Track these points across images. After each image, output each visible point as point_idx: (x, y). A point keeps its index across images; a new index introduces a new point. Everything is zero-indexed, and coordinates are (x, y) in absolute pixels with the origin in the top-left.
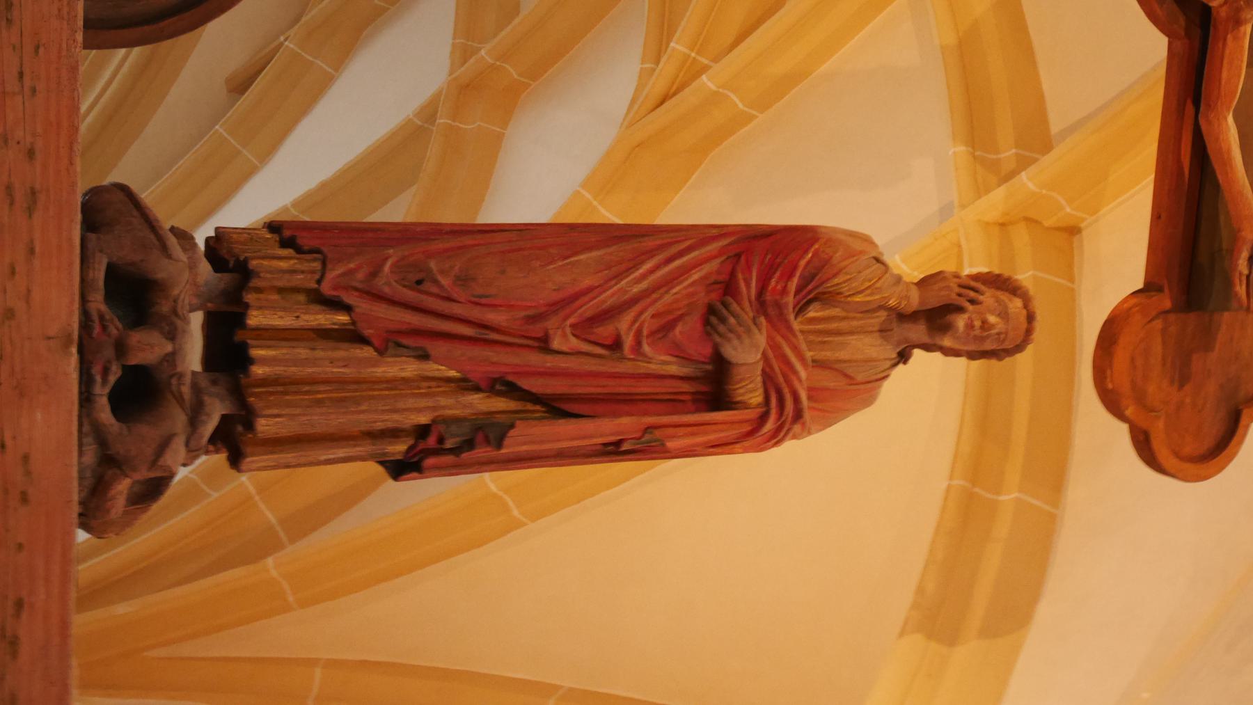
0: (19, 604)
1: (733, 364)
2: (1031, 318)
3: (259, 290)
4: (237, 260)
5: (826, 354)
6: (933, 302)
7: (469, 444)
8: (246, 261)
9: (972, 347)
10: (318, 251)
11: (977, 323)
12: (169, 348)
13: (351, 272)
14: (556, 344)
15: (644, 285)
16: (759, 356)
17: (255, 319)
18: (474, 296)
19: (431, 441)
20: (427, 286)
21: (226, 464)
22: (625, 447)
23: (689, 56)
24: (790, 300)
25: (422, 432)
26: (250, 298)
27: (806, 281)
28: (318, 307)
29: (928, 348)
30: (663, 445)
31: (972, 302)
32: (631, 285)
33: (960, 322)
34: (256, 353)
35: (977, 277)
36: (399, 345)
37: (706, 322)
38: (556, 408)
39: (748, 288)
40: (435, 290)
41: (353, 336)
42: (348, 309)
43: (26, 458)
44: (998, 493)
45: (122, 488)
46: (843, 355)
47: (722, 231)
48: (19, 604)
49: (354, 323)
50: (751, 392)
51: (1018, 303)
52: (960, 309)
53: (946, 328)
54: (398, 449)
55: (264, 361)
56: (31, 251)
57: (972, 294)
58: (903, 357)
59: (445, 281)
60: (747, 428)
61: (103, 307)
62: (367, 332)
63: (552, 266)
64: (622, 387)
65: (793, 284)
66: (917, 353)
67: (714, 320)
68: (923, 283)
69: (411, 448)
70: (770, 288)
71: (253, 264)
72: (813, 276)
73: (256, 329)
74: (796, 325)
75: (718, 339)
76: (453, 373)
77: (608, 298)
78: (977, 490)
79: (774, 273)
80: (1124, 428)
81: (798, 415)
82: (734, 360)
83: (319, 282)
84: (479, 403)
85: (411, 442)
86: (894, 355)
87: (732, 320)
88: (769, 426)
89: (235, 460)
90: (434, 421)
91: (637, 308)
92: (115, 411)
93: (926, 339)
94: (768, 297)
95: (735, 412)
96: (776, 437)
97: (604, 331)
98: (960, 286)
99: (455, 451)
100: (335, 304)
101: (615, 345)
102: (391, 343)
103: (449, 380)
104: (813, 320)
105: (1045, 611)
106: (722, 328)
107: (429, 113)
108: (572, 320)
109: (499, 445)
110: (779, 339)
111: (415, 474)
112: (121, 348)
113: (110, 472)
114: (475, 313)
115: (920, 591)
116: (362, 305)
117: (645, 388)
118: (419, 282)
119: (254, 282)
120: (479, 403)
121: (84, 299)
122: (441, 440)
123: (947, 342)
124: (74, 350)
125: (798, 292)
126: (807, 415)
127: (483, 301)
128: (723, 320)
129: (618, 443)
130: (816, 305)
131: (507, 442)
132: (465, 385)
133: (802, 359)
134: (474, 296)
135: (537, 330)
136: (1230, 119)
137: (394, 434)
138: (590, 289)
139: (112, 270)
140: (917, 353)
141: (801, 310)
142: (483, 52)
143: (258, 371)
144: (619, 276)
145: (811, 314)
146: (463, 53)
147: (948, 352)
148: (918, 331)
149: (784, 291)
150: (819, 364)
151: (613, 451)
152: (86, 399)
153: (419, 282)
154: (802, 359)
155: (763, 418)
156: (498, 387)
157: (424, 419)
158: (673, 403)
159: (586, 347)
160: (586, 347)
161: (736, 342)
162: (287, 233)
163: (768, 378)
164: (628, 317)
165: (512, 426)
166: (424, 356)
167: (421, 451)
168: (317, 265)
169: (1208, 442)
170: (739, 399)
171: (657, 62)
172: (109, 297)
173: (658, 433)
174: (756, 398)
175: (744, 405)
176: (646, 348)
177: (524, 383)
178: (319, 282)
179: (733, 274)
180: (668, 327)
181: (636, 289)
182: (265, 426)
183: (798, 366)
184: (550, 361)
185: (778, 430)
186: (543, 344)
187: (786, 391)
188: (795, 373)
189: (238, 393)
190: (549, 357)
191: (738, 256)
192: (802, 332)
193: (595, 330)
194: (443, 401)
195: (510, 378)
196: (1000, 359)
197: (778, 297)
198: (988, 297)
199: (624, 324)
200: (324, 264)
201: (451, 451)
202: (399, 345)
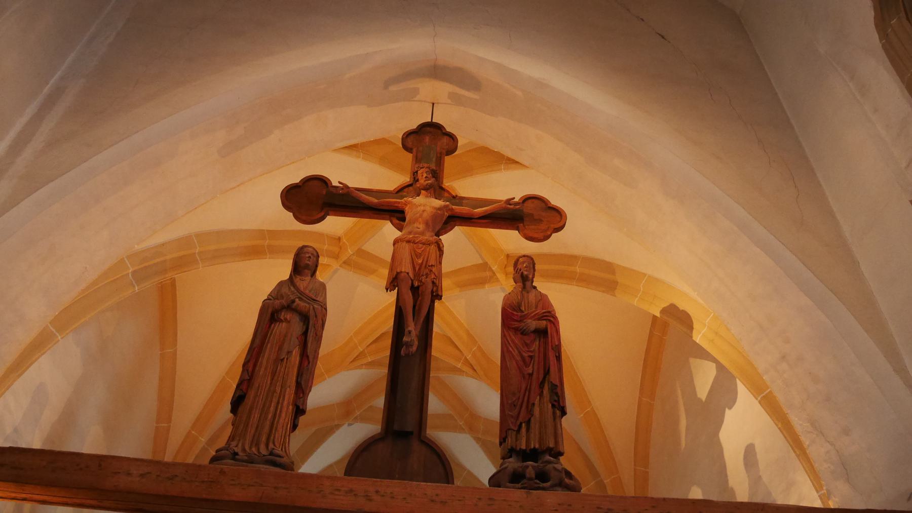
0: (599, 508)
2: (524, 256)
3: (516, 446)
4: (508, 452)
5: (534, 305)
6: (520, 279)
7: (557, 394)
8: (509, 449)
9: (532, 270)
10: (506, 432)
11: (526, 269)
12: (530, 467)
13: (512, 423)
14: (531, 372)
15: (516, 350)
16: (534, 322)
17: (524, 447)
19: (555, 403)
21: (563, 457)
22: (557, 355)
23: (462, 363)
24: (519, 314)
25: (553, 406)
26: (518, 448)
27: (514, 310)
28: (521, 433)
29: (533, 282)
30: (557, 345)
31: (520, 270)
32: (515, 353)
33: (525, 273)
34: (532, 447)
35: (514, 270)
36: (531, 411)
37: (525, 335)
38: (547, 372)
39: (516, 324)
40: (517, 401)
41: (528, 423)
42: (521, 424)
43: (559, 504)
45: (567, 480)
46: (534, 302)
47: (503, 336)
48: (599, 508)
49: (524, 422)
50: (543, 324)
51: (521, 259)
52: (522, 273)
53: (527, 276)
54: (558, 413)
55: (534, 445)
56: (505, 500)
57: (518, 270)
58: (535, 288)
59: (514, 399)
60: (552, 325)
61: (520, 484)
62: (527, 419)
64: (542, 355)
65: (515, 313)
66: (534, 284)
67: (524, 333)
68: (516, 282)
69: (558, 410)
71: (509, 447)
72: (514, 309)
73: (526, 446)
74: (526, 313)
75: (529, 331)
76: (538, 397)
77: (519, 358)
80: (554, 235)
81: (549, 312)
83: (514, 431)
84: (546, 391)
86: (534, 290)
87: (525, 328)
88: (552, 319)
89: (561, 454)
90: (551, 402)
91: (522, 352)
92: (547, 482)
93: (530, 282)
94: (519, 319)
95: (548, 328)
96: (555, 318)
97: (527, 360)
98: (516, 273)
99: (558, 397)
100: (520, 427)
101: (531, 357)
102: (530, 412)
103: (540, 399)
104: (525, 309)
105: (608, 258)
107: (478, 440)
108: (525, 368)
109: (557, 386)
110: (529, 317)
112: (530, 479)
114: (523, 391)
115: (603, 292)
116: (520, 419)
117: (542, 349)
118: (514, 405)
119: (514, 447)
120: (546, 391)
121: (519, 489)
122: (555, 401)
123: (531, 276)
124: (531, 491)
125: (517, 312)
126: (549, 310)
128: (525, 330)
129: (556, 356)
130: (521, 308)
131: (556, 384)
132: (541, 395)
133: (535, 311)
135: (527, 377)
136: (476, 210)
137: (554, 413)
138: (516, 363)
139: (509, 483)
140: (534, 284)
141: (523, 312)
142: (461, 424)
143: (537, 446)
144: (513, 356)
145: (523, 309)
146: (459, 429)
147: (533, 277)
148: (528, 284)
149: (517, 315)
150: (536, 307)
151: (559, 358)
152: (544, 489)
153: (514, 405)
154: (535, 311)
155: (550, 321)
156: (542, 386)
157: (550, 405)
158: (546, 343)
159: (531, 365)
160: (531, 365)
162: (502, 441)
163: (539, 319)
164: (524, 354)
165: (551, 382)
166: (534, 404)
168: (510, 431)
169: (557, 214)
170: (545, 326)
171: (464, 371)
172: (518, 483)
173: (554, 346)
174: (544, 322)
175: (547, 325)
176: (532, 349)
177: (541, 380)
178: (514, 431)
179: (513, 328)
180: (527, 345)
182: (552, 445)
183: (537, 312)
184: (535, 374)
185: (553, 317)
186: (531, 375)
187: (542, 315)
188: (539, 312)
189: (544, 452)
190: (534, 373)
191: (508, 327)
192: (528, 311)
194: (545, 400)
196: (535, 264)
198: (519, 266)
199: (525, 355)
200: (509, 429)
201: (558, 398)
202: (531, 411)
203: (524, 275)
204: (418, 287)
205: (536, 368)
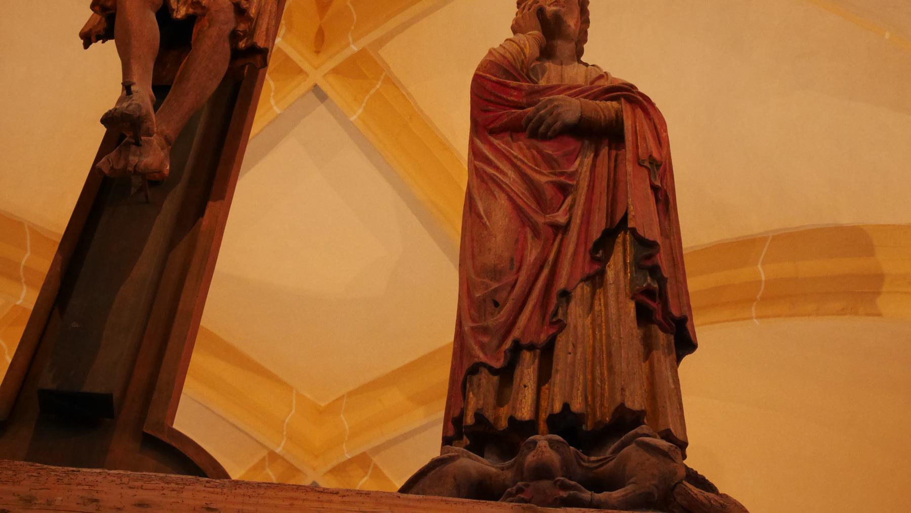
1: (581, 116)
7: (655, 271)
14: (561, 218)
18: (511, 269)
20: (500, 297)
32: (510, 177)
41: (547, 352)
44: (760, 281)
54: (662, 338)
60: (639, 112)
63: (488, 223)
69: (664, 330)
70: (516, 100)
78: (758, 297)
79: (503, 99)
82: (578, 114)
85: (655, 328)
97: (549, 192)
99: (662, 281)
105: (847, 219)
106: (549, 120)
109: (653, 245)
111: (688, 325)
113: (679, 499)
115: (842, 312)
118: (496, 304)
122: (649, 292)
123: (572, 22)
127: (516, 264)
134: (511, 269)
138: (510, 199)
143: (577, 406)
153: (496, 304)
156: (600, 254)
161: (560, 110)
167: (664, 318)
170: (614, 115)
181: (511, 174)
186: (561, 230)
193: (549, 198)
195: (590, 245)
197: (523, 93)
203: (548, 15)
204: (191, 20)
205: (578, 212)
